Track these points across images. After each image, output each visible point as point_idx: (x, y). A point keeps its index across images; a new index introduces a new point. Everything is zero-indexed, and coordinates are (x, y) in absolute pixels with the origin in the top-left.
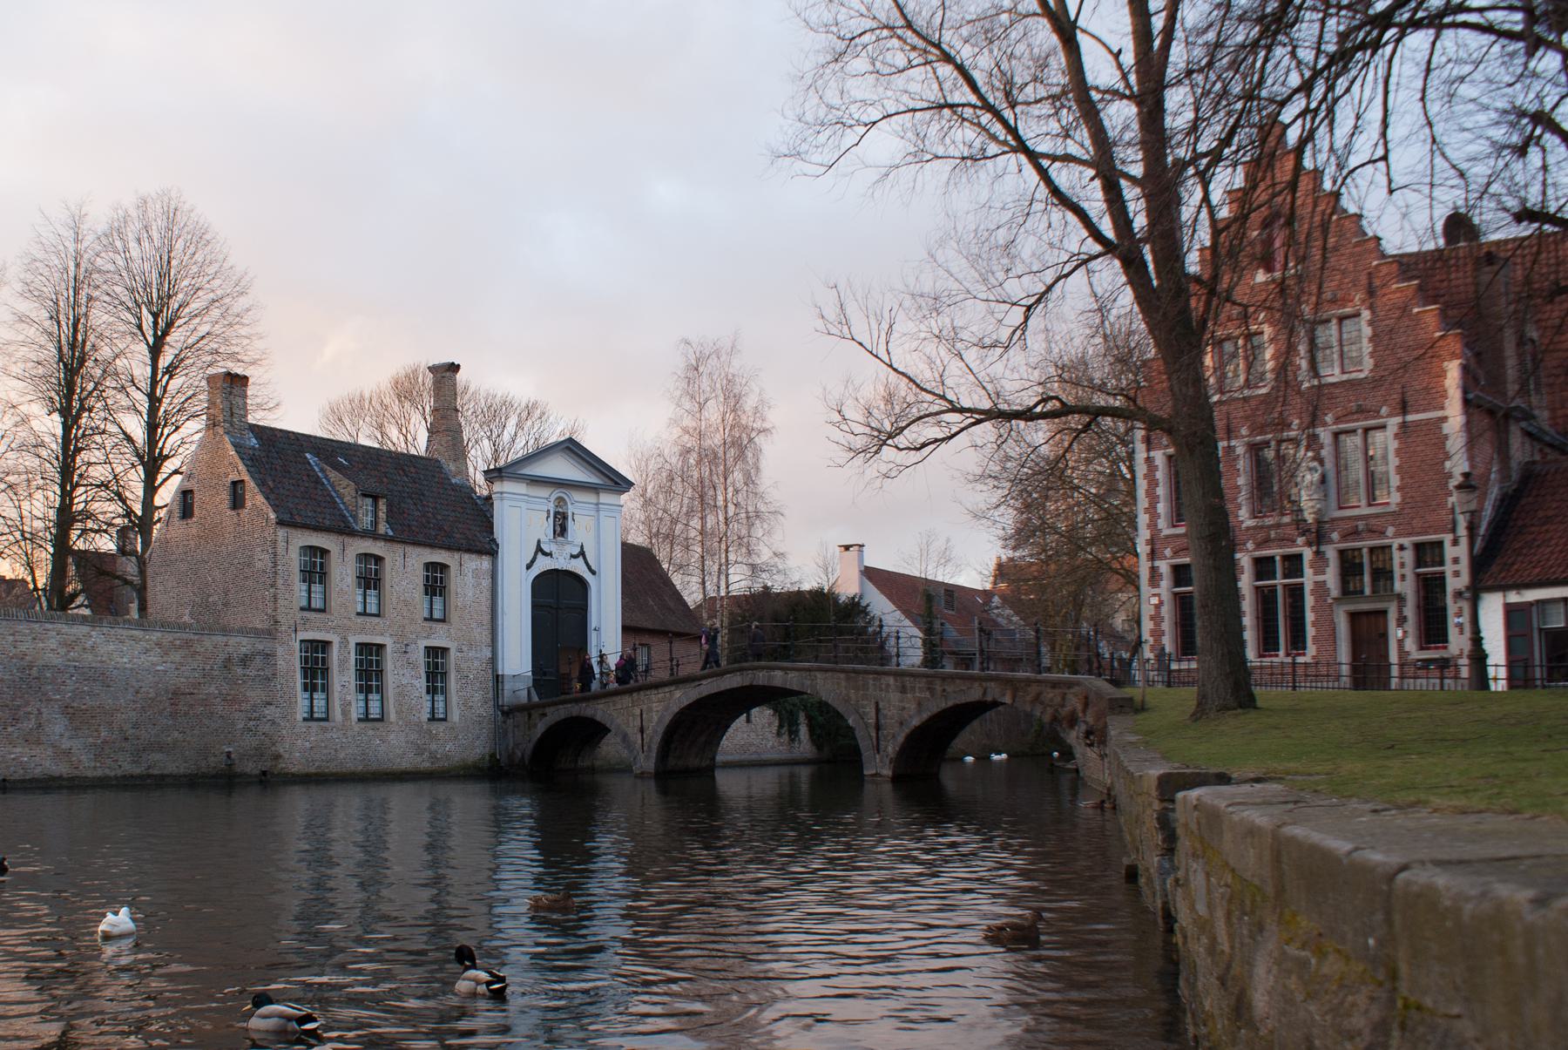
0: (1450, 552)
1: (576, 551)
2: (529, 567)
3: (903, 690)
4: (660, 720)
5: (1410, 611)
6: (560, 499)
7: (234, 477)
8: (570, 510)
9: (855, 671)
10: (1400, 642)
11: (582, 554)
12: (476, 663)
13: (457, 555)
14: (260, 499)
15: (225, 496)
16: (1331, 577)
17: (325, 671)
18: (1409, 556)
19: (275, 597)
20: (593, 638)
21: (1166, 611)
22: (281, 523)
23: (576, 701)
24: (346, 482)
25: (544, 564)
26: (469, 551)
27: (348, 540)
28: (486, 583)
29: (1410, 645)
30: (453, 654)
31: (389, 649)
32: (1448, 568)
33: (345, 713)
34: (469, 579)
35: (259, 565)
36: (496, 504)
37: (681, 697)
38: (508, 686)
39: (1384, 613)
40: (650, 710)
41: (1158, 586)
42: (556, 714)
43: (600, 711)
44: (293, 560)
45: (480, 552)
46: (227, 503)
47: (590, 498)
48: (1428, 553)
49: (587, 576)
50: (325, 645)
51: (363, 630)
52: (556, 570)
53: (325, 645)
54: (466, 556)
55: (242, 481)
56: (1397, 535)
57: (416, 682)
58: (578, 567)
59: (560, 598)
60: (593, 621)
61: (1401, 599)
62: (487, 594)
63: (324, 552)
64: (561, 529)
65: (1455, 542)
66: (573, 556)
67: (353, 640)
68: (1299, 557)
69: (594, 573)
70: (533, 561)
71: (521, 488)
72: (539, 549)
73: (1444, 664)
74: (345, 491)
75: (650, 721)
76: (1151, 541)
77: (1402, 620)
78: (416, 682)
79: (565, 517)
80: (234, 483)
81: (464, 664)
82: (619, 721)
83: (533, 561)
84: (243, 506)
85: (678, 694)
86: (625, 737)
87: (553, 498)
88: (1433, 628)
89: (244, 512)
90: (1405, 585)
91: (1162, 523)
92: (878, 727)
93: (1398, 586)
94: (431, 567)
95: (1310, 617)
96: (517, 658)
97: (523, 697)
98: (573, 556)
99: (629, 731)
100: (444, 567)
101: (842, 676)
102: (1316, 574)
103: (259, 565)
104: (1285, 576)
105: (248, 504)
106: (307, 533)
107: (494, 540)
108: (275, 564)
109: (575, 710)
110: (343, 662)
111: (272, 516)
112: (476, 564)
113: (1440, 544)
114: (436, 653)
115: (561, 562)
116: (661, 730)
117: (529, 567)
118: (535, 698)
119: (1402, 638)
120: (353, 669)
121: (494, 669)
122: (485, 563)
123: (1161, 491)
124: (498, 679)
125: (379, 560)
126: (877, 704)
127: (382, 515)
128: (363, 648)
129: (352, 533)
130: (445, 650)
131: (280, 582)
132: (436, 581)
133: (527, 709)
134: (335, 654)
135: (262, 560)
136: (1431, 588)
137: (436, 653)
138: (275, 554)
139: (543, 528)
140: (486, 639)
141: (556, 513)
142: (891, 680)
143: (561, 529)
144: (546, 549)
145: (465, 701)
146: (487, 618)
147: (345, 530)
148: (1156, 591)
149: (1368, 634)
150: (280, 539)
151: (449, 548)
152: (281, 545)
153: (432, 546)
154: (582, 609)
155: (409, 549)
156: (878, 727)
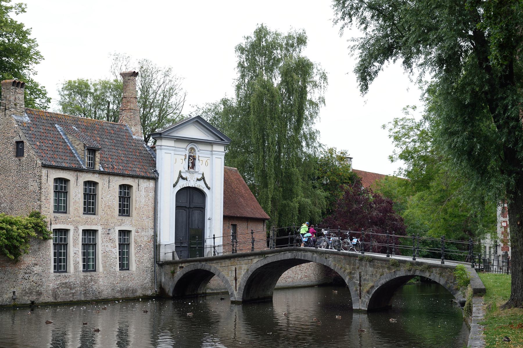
1: (200, 177)
2: (174, 186)
6: (192, 149)
7: (17, 139)
9: (349, 255)
11: (203, 178)
12: (146, 238)
13: (137, 180)
14: (32, 152)
15: (12, 148)
17: (66, 245)
19: (40, 206)
20: (207, 223)
22: (44, 166)
23: (200, 261)
25: (182, 184)
26: (143, 178)
27: (79, 174)
28: (152, 194)
30: (133, 234)
31: (100, 232)
33: (76, 268)
34: (143, 193)
35: (31, 188)
36: (158, 152)
37: (256, 263)
38: (162, 251)
42: (187, 268)
43: (213, 267)
44: (50, 186)
45: (149, 178)
46: (13, 153)
47: (209, 148)
49: (205, 190)
50: (66, 231)
51: (86, 223)
52: (189, 187)
53: (66, 231)
54: (141, 181)
57: (113, 250)
58: (201, 185)
59: (190, 201)
60: (208, 214)
62: (152, 201)
63: (66, 181)
66: (198, 180)
67: (81, 228)
69: (209, 188)
70: (177, 183)
71: (171, 143)
72: (180, 176)
74: (78, 147)
75: (240, 274)
78: (113, 250)
79: (194, 159)
80: (17, 143)
81: (139, 240)
83: (177, 183)
85: (255, 261)
86: (227, 282)
87: (188, 148)
94: (122, 187)
96: (168, 236)
97: (169, 257)
98: (198, 180)
99: (229, 278)
100: (129, 187)
101: (342, 257)
103: (31, 188)
105: (26, 155)
106: (58, 171)
107: (156, 171)
108: (40, 188)
109: (199, 266)
110: (75, 240)
111: (39, 162)
112: (147, 185)
114: (124, 234)
115: (192, 183)
116: (246, 279)
117: (174, 186)
118: (177, 258)
120: (81, 243)
121: (155, 241)
122: (152, 184)
124: (157, 247)
125: (95, 184)
127: (97, 160)
128: (85, 231)
129: (81, 170)
130: (129, 232)
131: (43, 198)
132: (125, 196)
133: (172, 263)
134: (71, 236)
135: (33, 186)
137: (124, 234)
138: (41, 183)
139: (183, 165)
140: (151, 225)
141: (190, 156)
144: (184, 175)
145: (140, 259)
146: (151, 214)
147: (79, 170)
150: (43, 174)
151: (133, 177)
152: (44, 178)
153: (123, 176)
154: (202, 209)
155: (112, 178)
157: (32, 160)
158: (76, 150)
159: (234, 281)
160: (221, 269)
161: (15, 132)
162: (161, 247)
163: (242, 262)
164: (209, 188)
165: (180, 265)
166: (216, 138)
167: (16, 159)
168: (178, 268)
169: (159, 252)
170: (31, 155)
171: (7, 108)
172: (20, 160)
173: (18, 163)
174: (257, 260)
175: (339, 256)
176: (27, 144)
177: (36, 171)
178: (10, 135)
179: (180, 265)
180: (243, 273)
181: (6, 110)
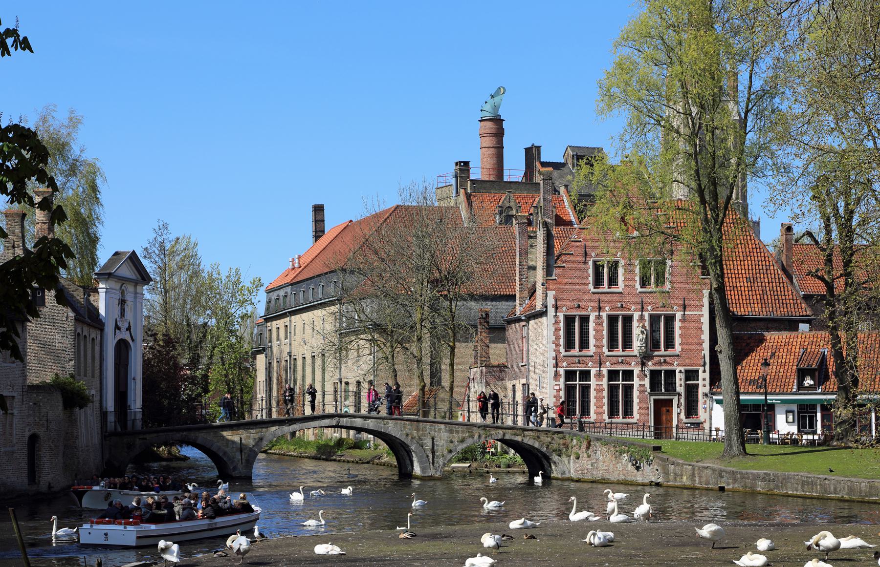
0: (701, 375)
3: (451, 432)
5: (682, 401)
10: (679, 414)
11: (129, 329)
16: (647, 382)
18: (683, 376)
29: (683, 416)
32: (700, 382)
39: (671, 400)
48: (691, 375)
56: (678, 366)
61: (679, 395)
64: (122, 314)
65: (704, 371)
69: (133, 340)
73: (698, 424)
76: (556, 358)
77: (679, 405)
88: (691, 409)
90: (680, 389)
91: (562, 350)
92: (433, 452)
95: (636, 400)
102: (640, 380)
113: (697, 371)
118: (119, 429)
119: (678, 413)
123: (562, 333)
124: (104, 414)
126: (433, 439)
133: (114, 434)
136: (691, 392)
142: (442, 426)
143: (122, 314)
148: (557, 383)
149: (662, 408)
156: (433, 452)
159: (238, 454)
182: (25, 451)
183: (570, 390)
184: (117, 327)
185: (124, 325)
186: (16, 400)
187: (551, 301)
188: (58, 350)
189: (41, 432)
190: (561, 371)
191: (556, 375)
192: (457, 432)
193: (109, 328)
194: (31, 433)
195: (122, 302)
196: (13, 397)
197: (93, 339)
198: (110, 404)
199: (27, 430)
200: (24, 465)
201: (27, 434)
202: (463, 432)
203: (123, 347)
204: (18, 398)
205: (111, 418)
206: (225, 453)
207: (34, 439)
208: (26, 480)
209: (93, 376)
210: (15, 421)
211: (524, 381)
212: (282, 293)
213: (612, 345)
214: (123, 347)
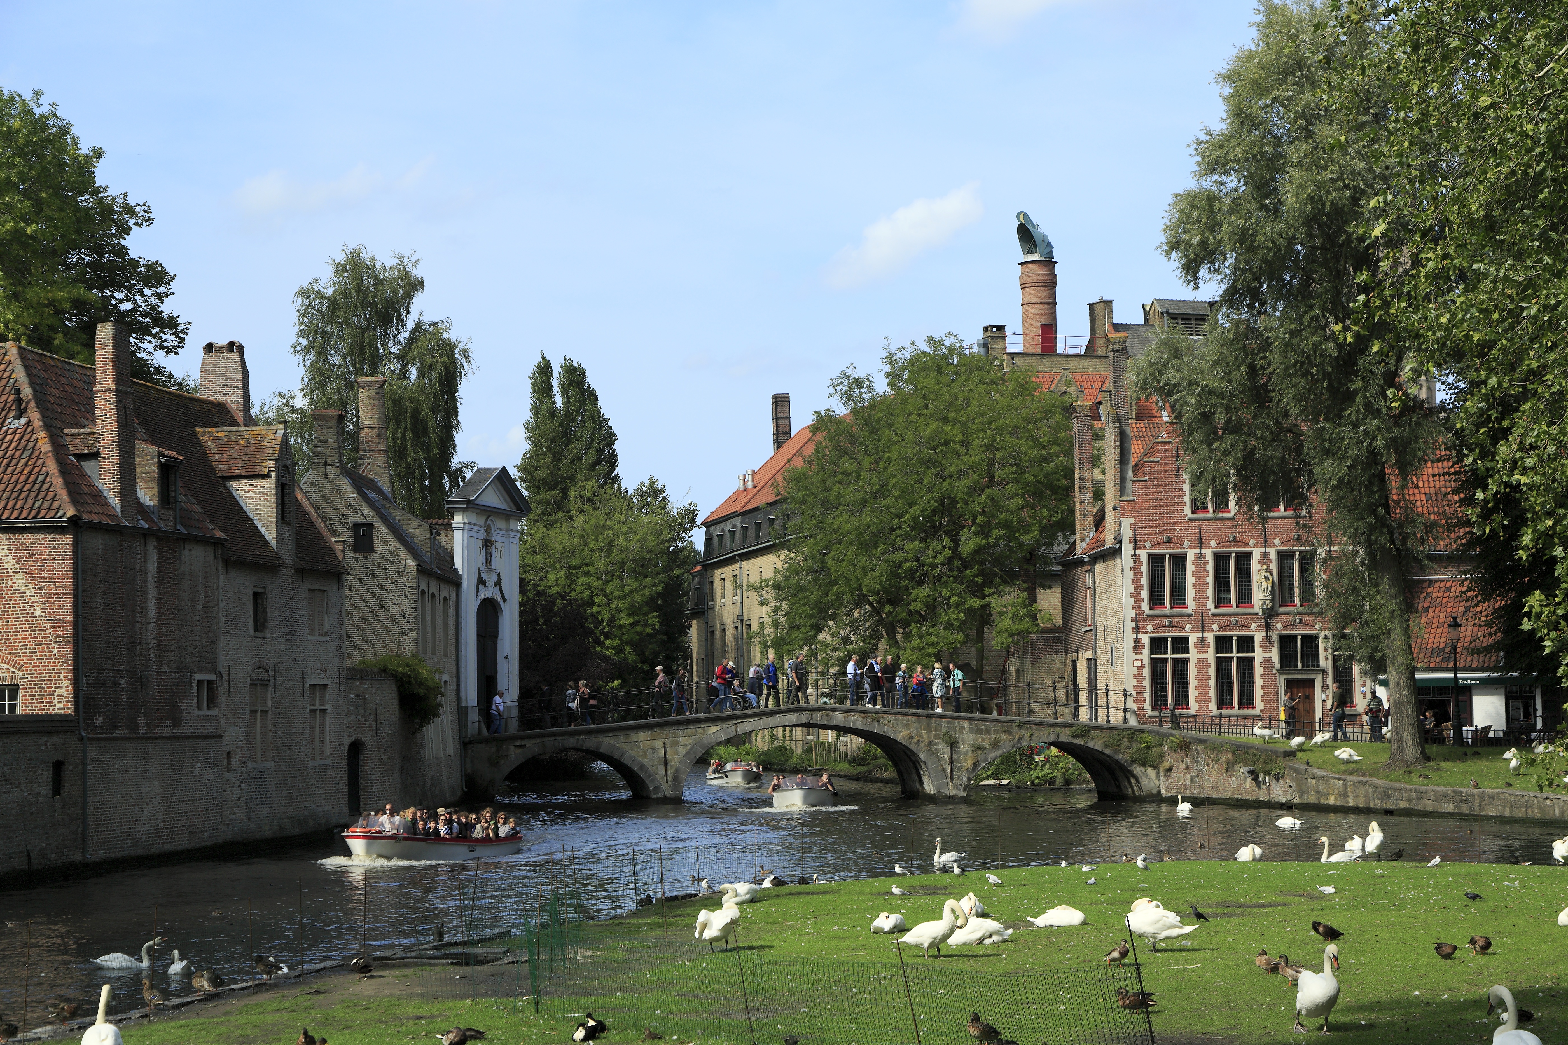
4: (688, 753)
7: (360, 519)
8: (495, 537)
10: (1324, 702)
16: (1274, 654)
21: (1146, 672)
24: (415, 522)
35: (394, 609)
39: (1312, 682)
40: (676, 744)
41: (1141, 653)
49: (501, 603)
55: (370, 526)
61: (1324, 672)
68: (1252, 638)
69: (505, 600)
75: (676, 753)
76: (1136, 619)
77: (1325, 687)
80: (356, 526)
82: (633, 753)
84: (372, 550)
89: (372, 557)
91: (1145, 606)
93: (1322, 663)
95: (1258, 682)
101: (913, 718)
102: (1264, 651)
104: (1238, 652)
105: (379, 549)
123: (1144, 581)
142: (966, 724)
148: (1139, 656)
157: (395, 559)
158: (414, 536)
160: (626, 747)
161: (351, 506)
162: (469, 709)
163: (680, 733)
164: (505, 600)
165: (518, 743)
166: (512, 505)
167: (357, 555)
168: (512, 748)
169: (466, 721)
170: (392, 549)
171: (329, 462)
172: (366, 558)
173: (361, 562)
174: (719, 728)
175: (906, 718)
176: (381, 530)
177: (404, 579)
178: (340, 512)
179: (518, 743)
180: (683, 751)
181: (326, 464)
182: (344, 765)
183: (1158, 667)
184: (481, 582)
185: (491, 579)
186: (329, 690)
187: (1127, 534)
188: (393, 615)
189: (368, 738)
190: (1145, 639)
191: (1137, 645)
192: (988, 732)
193: (468, 583)
194: (352, 739)
195: (488, 544)
196: (325, 686)
197: (445, 599)
198: (471, 695)
199: (346, 734)
200: (343, 786)
201: (347, 741)
202: (996, 732)
203: (489, 611)
204: (332, 688)
205: (473, 716)
206: (642, 767)
207: (356, 748)
208: (346, 810)
209: (446, 655)
210: (328, 720)
211: (1089, 654)
212: (728, 526)
213: (1220, 601)
214: (489, 611)
